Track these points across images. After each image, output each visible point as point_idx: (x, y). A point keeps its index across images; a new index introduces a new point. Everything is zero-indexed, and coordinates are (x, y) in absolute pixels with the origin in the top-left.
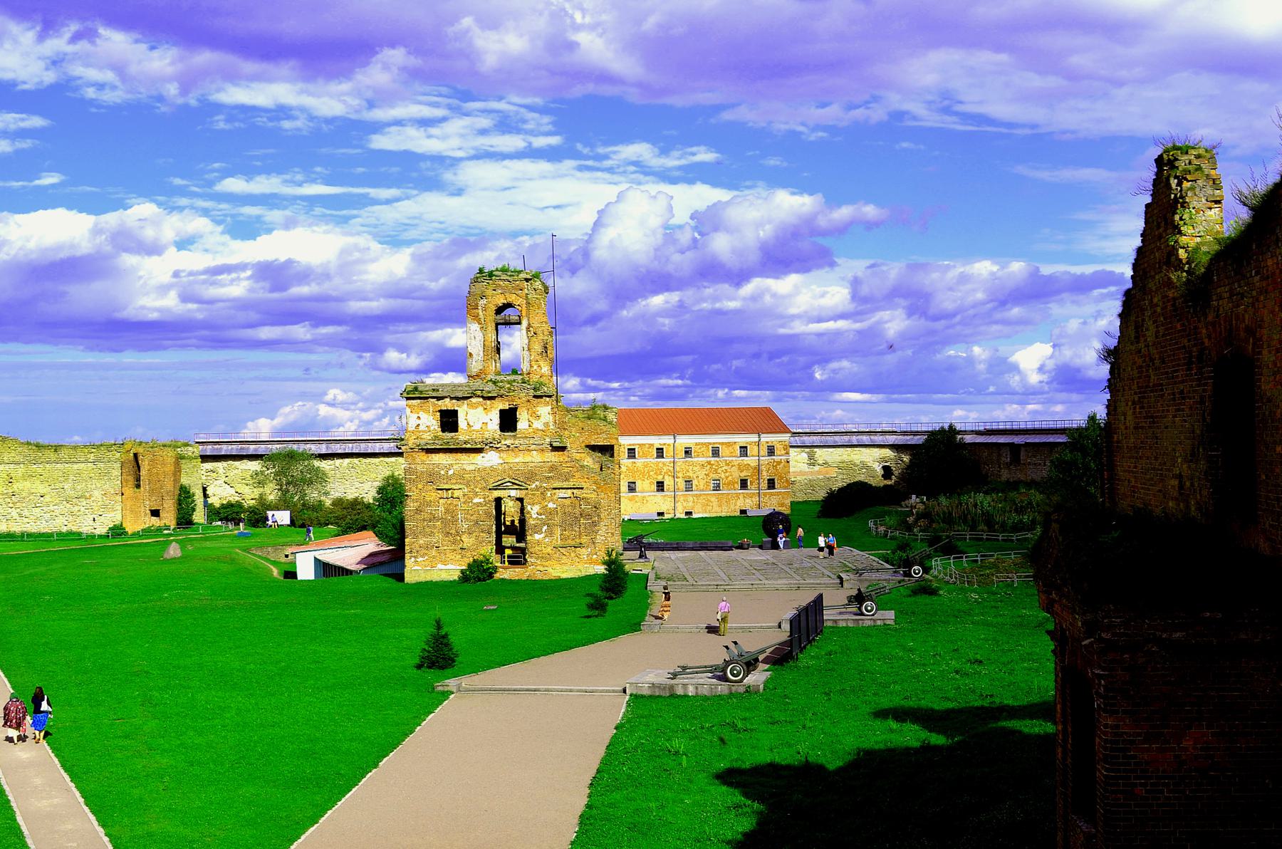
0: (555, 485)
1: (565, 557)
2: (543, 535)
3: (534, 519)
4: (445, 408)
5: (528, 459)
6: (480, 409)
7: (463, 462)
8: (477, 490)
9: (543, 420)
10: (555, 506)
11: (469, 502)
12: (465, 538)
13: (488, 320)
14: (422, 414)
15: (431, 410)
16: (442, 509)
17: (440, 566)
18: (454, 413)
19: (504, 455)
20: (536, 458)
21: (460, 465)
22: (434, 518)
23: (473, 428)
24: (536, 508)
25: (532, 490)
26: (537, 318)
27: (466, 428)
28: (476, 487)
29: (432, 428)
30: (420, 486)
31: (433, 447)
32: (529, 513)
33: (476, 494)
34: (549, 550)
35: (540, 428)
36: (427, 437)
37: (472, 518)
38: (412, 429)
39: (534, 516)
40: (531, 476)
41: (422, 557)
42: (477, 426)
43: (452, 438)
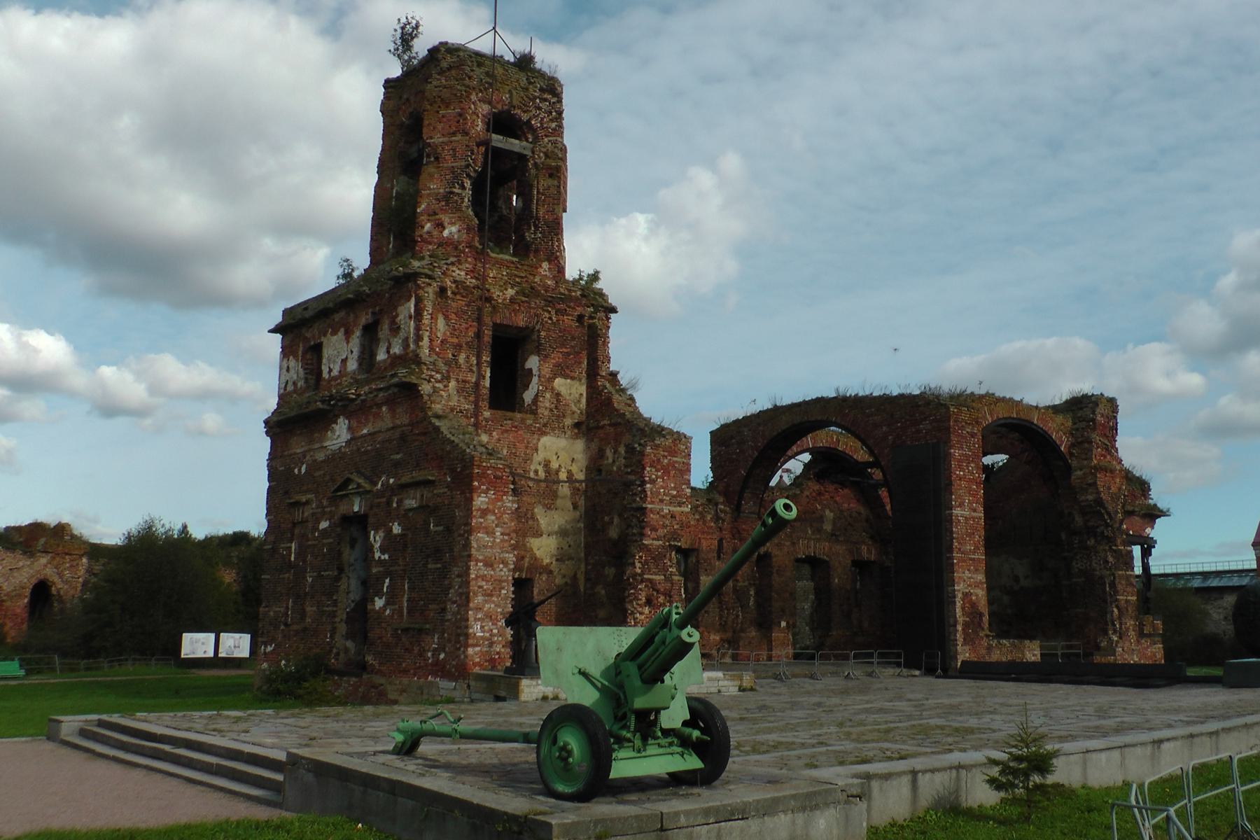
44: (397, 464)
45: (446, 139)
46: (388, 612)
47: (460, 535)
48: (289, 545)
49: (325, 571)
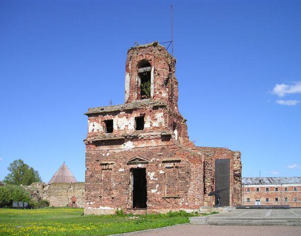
2: (156, 190)
3: (151, 181)
9: (158, 121)
10: (163, 172)
14: (95, 123)
17: (101, 207)
18: (112, 121)
20: (153, 143)
22: (99, 180)
23: (120, 129)
24: (153, 174)
25: (150, 163)
33: (120, 167)
34: (159, 199)
35: (157, 126)
40: (150, 154)
41: (93, 202)
42: (122, 128)
46: (158, 193)
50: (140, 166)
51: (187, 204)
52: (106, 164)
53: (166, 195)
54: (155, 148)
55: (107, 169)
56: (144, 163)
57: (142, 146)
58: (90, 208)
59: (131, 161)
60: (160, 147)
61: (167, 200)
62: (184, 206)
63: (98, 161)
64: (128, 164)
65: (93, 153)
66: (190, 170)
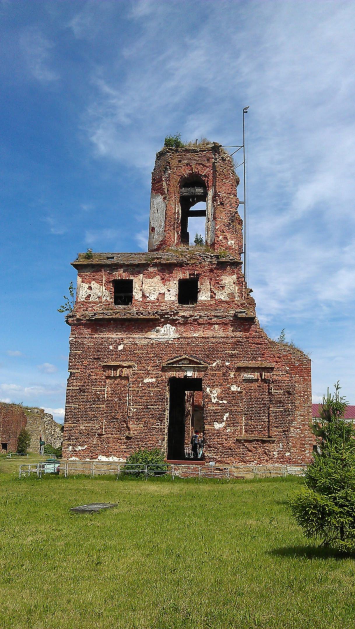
0: (240, 364)
1: (250, 453)
2: (223, 424)
4: (119, 278)
5: (209, 333)
6: (157, 279)
7: (135, 336)
8: (149, 368)
9: (227, 290)
10: (239, 389)
11: (139, 382)
12: (131, 425)
13: (172, 189)
14: (94, 285)
15: (104, 280)
16: (107, 389)
17: (102, 458)
19: (182, 329)
21: (131, 340)
22: (98, 399)
23: (148, 299)
25: (212, 369)
26: (224, 188)
27: (141, 300)
28: (148, 365)
29: (104, 299)
30: (86, 363)
31: (101, 317)
32: (208, 396)
33: (148, 374)
34: (231, 443)
36: (98, 309)
37: (142, 400)
38: (82, 300)
39: (214, 401)
43: (124, 309)
44: (232, 356)
45: (227, 196)
46: (229, 430)
47: (301, 396)
48: (104, 388)
49: (152, 405)
50: (189, 374)
51: (288, 454)
52: (115, 368)
53: (244, 435)
54: (221, 340)
55: (115, 378)
56: (199, 370)
57: (195, 335)
58: (74, 458)
59: (173, 363)
60: (231, 341)
61: (247, 444)
62: (283, 460)
63: (99, 359)
64: (164, 369)
65: (88, 343)
66: (294, 388)
